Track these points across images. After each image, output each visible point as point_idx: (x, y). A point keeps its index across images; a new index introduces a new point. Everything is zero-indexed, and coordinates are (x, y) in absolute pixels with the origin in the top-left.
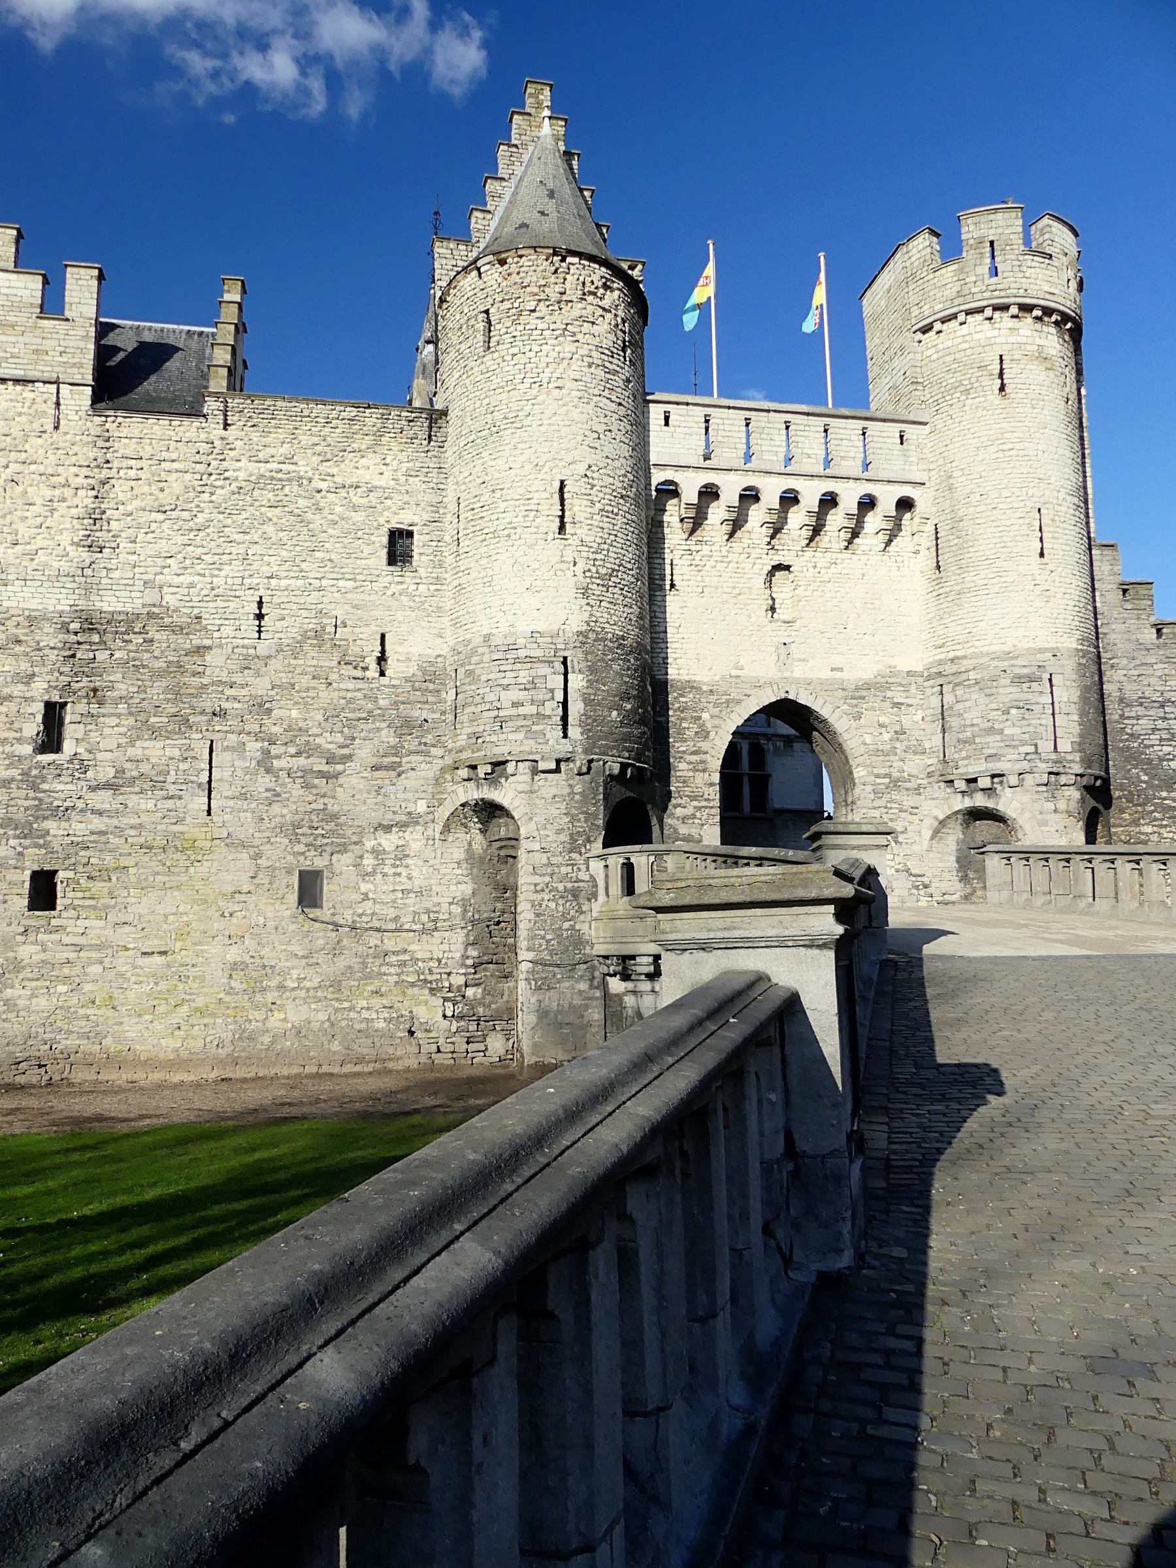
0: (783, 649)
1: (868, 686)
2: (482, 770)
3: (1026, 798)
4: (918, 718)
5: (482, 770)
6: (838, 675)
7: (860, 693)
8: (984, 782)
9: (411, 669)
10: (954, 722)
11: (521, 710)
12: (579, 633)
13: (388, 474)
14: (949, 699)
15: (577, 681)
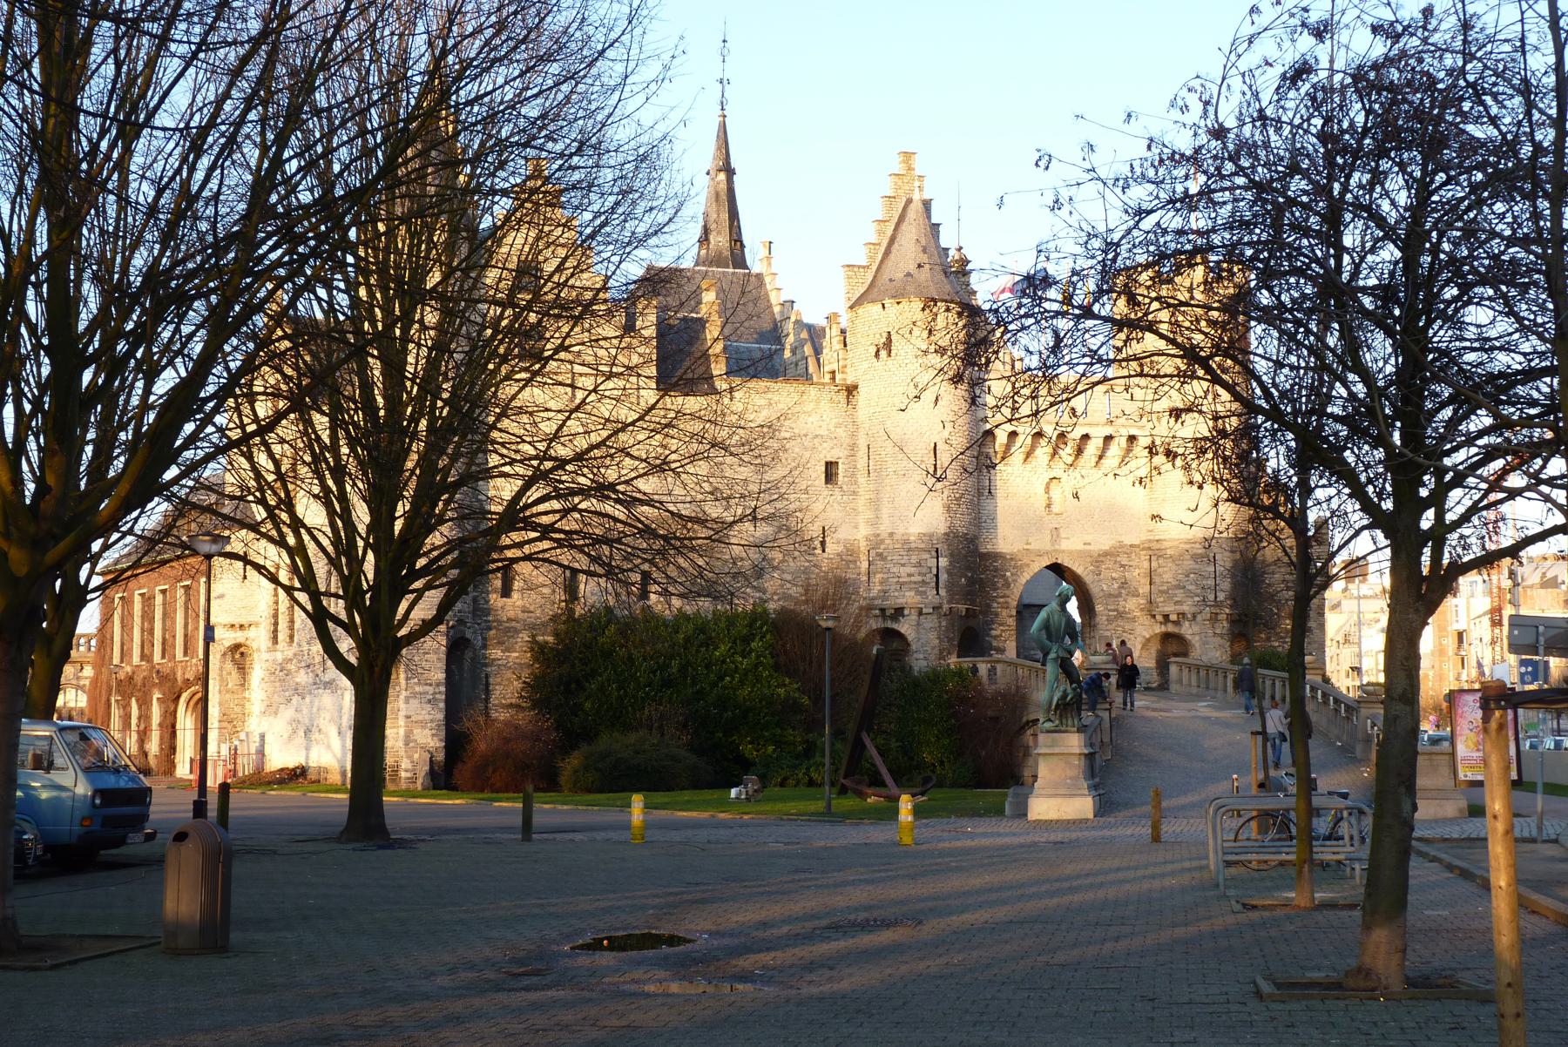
0: (1055, 533)
1: (1106, 554)
2: (888, 613)
3: (1196, 629)
4: (1135, 574)
5: (888, 613)
6: (1087, 547)
7: (1100, 559)
8: (1173, 617)
9: (840, 548)
10: (1157, 579)
11: (913, 579)
12: (945, 534)
13: (824, 427)
14: (1154, 564)
15: (943, 562)
